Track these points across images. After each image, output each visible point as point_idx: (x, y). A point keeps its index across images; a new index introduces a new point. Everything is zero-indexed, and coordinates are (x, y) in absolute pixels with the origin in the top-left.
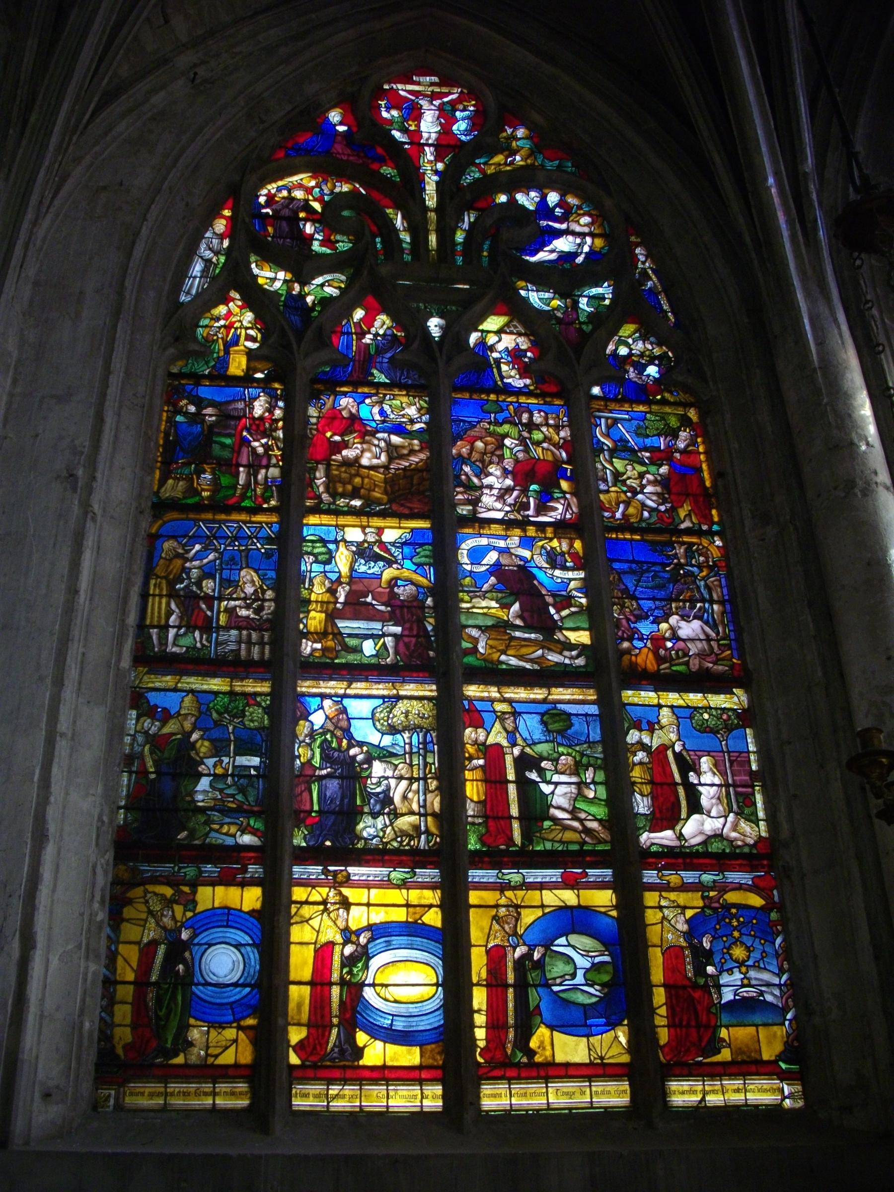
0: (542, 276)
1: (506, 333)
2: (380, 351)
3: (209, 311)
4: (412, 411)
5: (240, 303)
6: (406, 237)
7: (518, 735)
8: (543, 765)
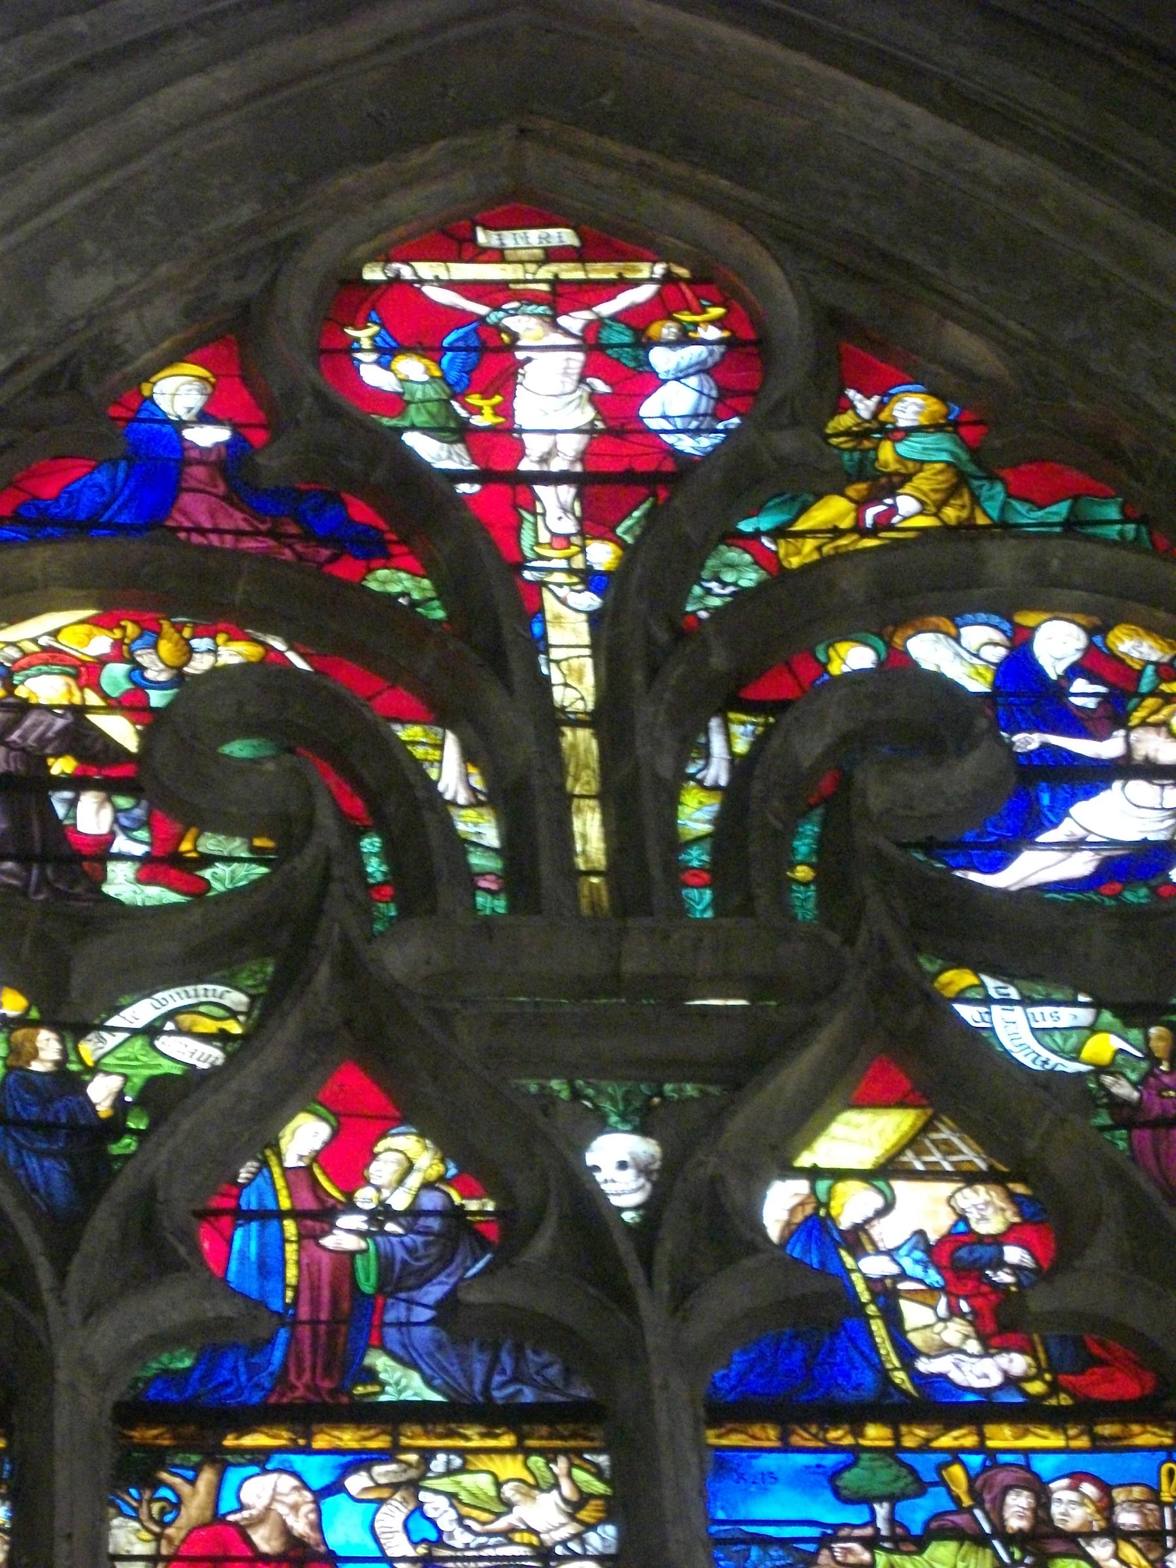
1: (912, 1175)
2: (398, 1278)
4: (545, 1515)
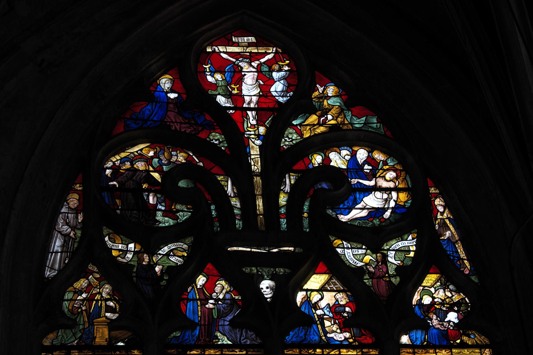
0: (355, 233)
2: (222, 315)
3: (72, 285)
5: (98, 276)
6: (235, 202)
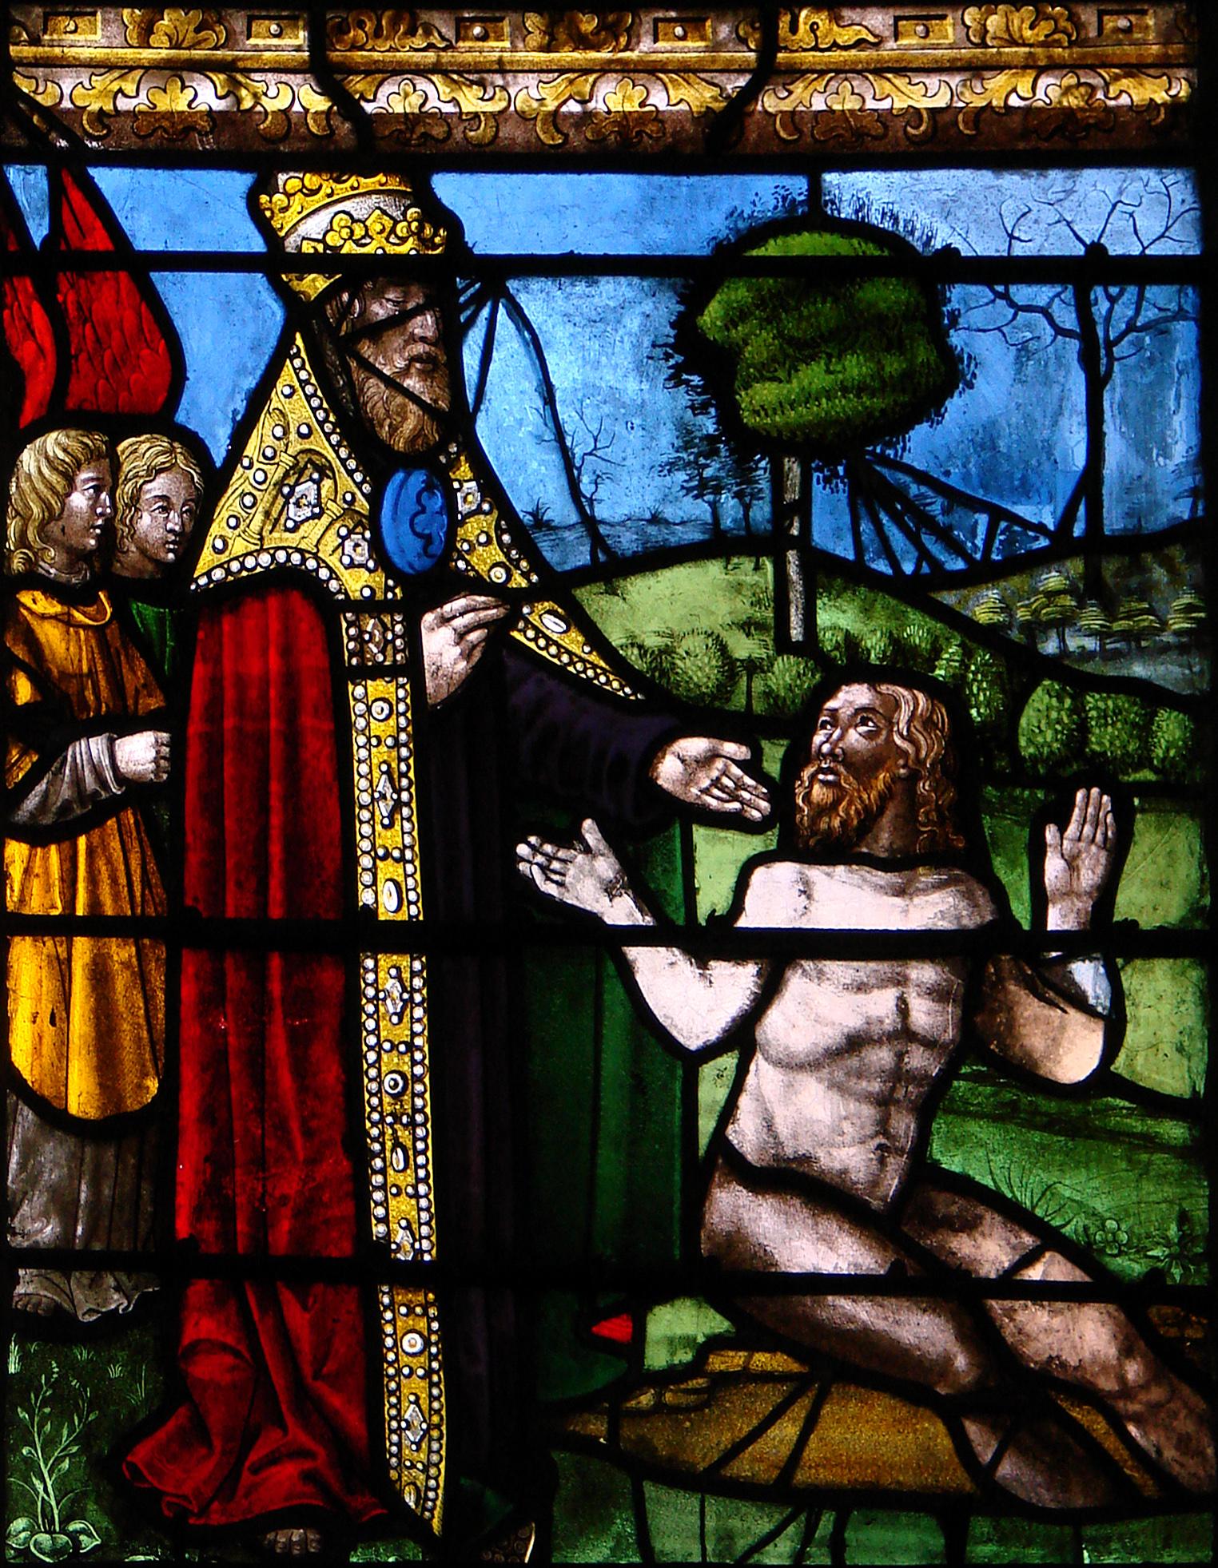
7: (468, 494)
8: (669, 770)
